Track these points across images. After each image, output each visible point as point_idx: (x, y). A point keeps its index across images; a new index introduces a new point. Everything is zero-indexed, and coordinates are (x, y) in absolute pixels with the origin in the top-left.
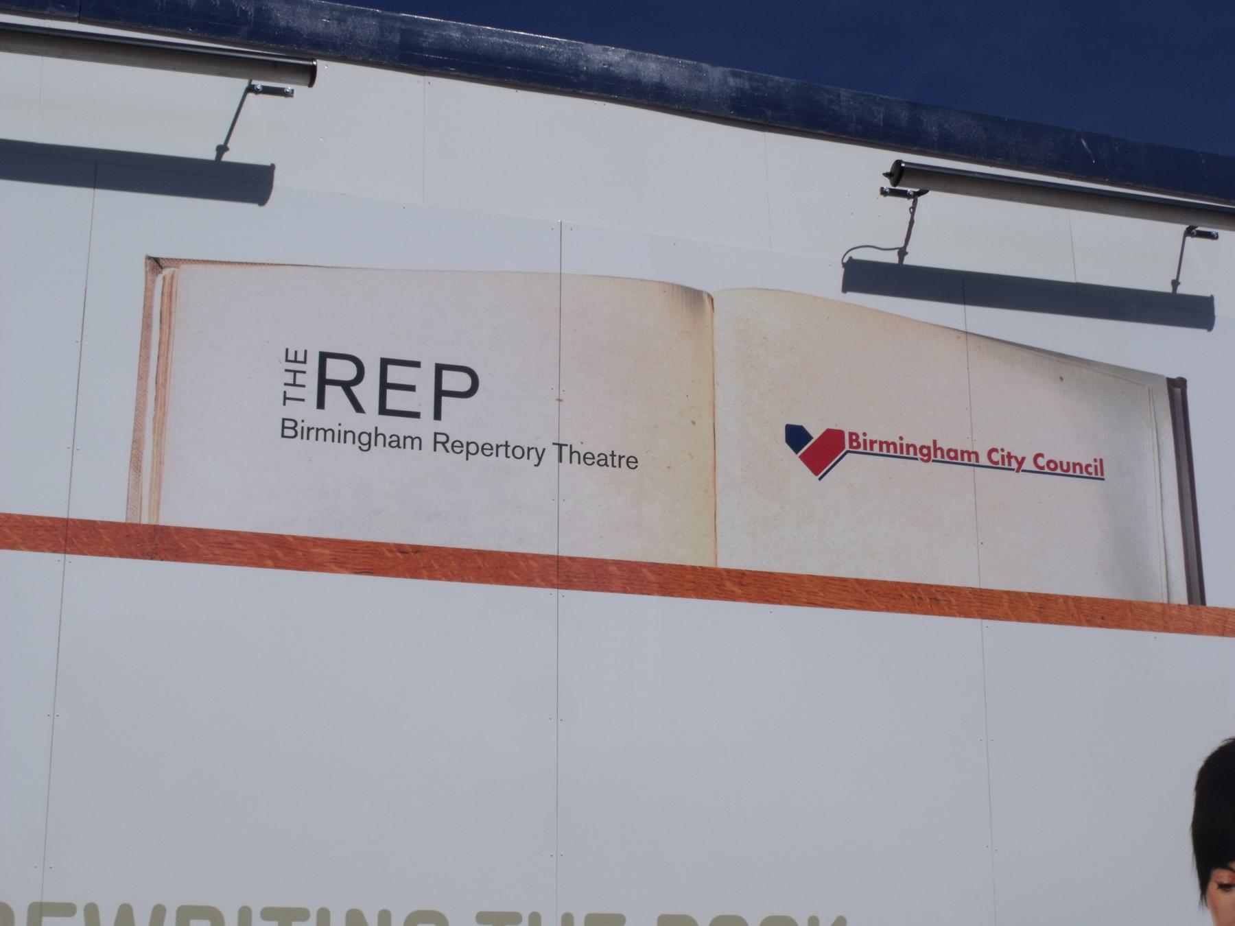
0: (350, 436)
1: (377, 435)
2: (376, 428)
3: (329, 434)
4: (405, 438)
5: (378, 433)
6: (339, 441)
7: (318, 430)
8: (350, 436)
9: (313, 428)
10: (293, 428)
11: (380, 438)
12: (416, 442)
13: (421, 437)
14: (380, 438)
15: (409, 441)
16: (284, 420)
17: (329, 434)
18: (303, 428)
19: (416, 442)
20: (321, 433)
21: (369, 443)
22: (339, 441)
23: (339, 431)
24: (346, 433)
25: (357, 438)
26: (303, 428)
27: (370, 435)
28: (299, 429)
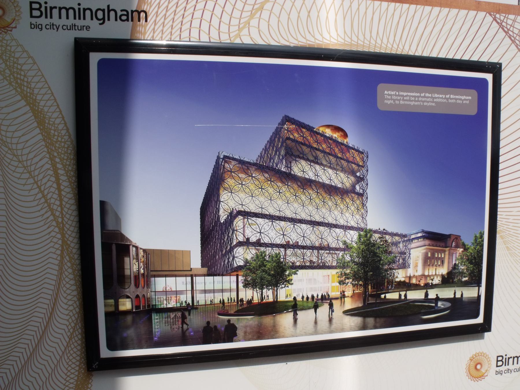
0: (88, 13)
1: (109, 11)
2: (108, 6)
3: (71, 12)
4: (132, 12)
5: (111, 8)
8: (88, 13)
9: (55, 7)
10: (39, 9)
11: (112, 14)
14: (112, 14)
16: (31, 3)
17: (71, 12)
18: (46, 8)
20: (64, 12)
21: (104, 19)
23: (79, 9)
25: (94, 15)
26: (46, 8)
27: (103, 11)
28: (43, 9)
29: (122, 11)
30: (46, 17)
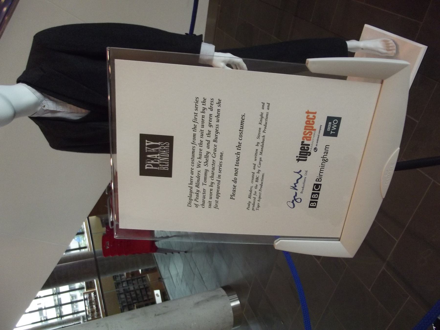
0: (323, 164)
1: (324, 157)
3: (322, 169)
5: (323, 157)
6: (324, 167)
7: (320, 172)
8: (323, 164)
10: (319, 179)
11: (325, 156)
12: (327, 147)
13: (326, 145)
14: (325, 156)
15: (326, 149)
17: (322, 169)
18: (319, 177)
19: (327, 147)
20: (321, 172)
22: (324, 167)
23: (321, 166)
24: (322, 165)
26: (319, 177)
28: (319, 178)
29: (324, 154)
30: (322, 177)
